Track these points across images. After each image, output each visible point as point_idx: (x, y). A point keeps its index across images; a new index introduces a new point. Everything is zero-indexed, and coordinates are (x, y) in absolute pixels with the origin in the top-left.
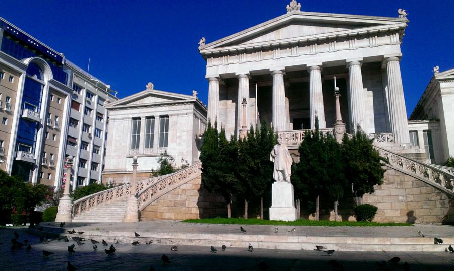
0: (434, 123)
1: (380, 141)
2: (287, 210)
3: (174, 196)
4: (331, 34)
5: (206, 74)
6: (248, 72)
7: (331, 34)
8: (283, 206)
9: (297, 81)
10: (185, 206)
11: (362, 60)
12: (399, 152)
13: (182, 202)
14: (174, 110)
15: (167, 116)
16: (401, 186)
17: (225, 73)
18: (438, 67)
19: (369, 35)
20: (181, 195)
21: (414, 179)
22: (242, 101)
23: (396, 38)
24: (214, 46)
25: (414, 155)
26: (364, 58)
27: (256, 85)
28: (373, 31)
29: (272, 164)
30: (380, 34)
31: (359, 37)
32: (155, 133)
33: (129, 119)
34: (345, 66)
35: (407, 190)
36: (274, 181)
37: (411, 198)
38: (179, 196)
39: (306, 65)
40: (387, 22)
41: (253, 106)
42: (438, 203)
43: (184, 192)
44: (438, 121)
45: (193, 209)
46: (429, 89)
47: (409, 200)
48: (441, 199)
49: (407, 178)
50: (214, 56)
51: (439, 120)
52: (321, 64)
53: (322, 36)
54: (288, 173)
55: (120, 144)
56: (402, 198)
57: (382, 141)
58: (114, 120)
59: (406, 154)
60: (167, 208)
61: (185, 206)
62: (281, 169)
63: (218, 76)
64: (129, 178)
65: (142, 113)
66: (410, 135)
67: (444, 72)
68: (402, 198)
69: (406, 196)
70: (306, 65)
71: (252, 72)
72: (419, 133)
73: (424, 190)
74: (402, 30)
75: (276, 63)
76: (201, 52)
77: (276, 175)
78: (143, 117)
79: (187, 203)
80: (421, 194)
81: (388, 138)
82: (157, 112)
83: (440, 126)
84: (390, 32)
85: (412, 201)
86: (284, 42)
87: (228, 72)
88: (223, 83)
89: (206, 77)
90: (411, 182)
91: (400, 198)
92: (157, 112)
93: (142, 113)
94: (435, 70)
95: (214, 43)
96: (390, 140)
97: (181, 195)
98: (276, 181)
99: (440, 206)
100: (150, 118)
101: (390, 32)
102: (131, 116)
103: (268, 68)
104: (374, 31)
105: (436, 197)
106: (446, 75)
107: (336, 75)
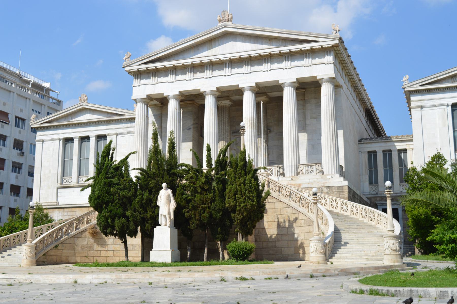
1: (309, 173)
4: (263, 51)
5: (132, 95)
7: (263, 51)
9: (230, 102)
11: (295, 80)
12: (322, 184)
13: (89, 245)
14: (112, 129)
18: (407, 76)
19: (302, 54)
21: (306, 218)
23: (330, 58)
24: (140, 63)
25: (336, 188)
26: (297, 79)
32: (90, 158)
33: (60, 140)
39: (238, 85)
41: (190, 129)
52: (254, 85)
53: (254, 53)
55: (50, 171)
57: (311, 173)
58: (43, 141)
59: (329, 187)
63: (145, 97)
64: (60, 213)
65: (76, 133)
66: (384, 154)
70: (238, 85)
72: (393, 153)
74: (336, 47)
75: (207, 83)
77: (161, 220)
78: (76, 138)
80: (309, 232)
81: (316, 169)
82: (92, 132)
84: (324, 51)
88: (155, 102)
89: (133, 97)
92: (92, 132)
93: (76, 133)
94: (404, 80)
96: (318, 171)
98: (160, 225)
100: (84, 139)
101: (324, 51)
102: (62, 136)
103: (198, 88)
104: (307, 48)
107: (270, 97)
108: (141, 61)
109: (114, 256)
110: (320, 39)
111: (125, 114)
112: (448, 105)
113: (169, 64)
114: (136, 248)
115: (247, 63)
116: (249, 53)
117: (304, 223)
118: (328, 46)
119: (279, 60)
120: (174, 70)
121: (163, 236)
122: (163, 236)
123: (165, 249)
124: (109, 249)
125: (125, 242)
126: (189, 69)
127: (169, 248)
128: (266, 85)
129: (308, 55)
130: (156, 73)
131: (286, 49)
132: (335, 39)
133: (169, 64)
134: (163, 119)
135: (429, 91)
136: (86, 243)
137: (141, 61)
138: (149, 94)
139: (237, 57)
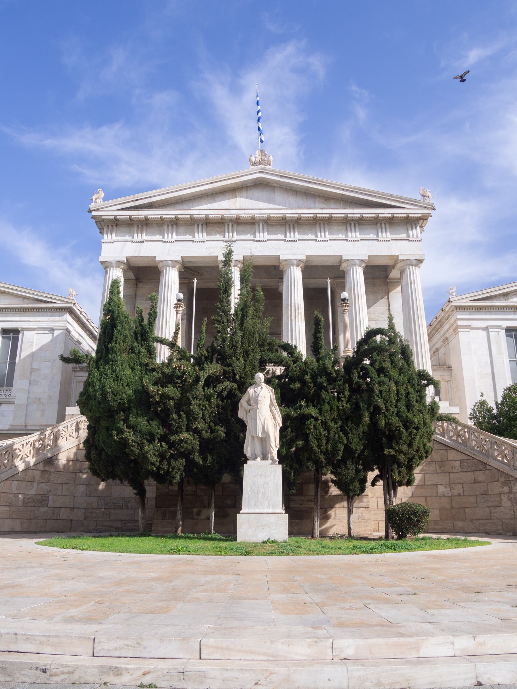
0: (444, 370)
2: (272, 518)
3: (24, 484)
4: (320, 211)
5: (100, 255)
6: (180, 259)
8: (265, 511)
10: (47, 506)
14: (30, 321)
15: (16, 331)
16: (443, 468)
17: (136, 255)
19: (377, 223)
20: (39, 483)
21: (464, 457)
22: (176, 302)
24: (120, 207)
26: (369, 256)
27: (195, 281)
28: (384, 215)
29: (243, 426)
30: (391, 222)
31: (360, 223)
34: (339, 266)
35: (451, 474)
36: (246, 460)
37: (458, 490)
38: (35, 484)
39: (279, 257)
40: (404, 206)
42: (505, 498)
43: (46, 476)
44: (449, 367)
45: (62, 510)
46: (438, 320)
47: (455, 492)
48: (510, 492)
49: (452, 455)
50: (115, 224)
51: (451, 367)
52: (303, 258)
53: (307, 212)
54: (275, 444)
56: (444, 490)
60: (7, 508)
61: (47, 506)
62: (260, 435)
67: (463, 297)
68: (444, 490)
69: (450, 485)
70: (279, 257)
71: (186, 260)
73: (481, 476)
76: (94, 213)
79: (51, 497)
80: (476, 482)
83: (451, 375)
85: (459, 495)
86: (245, 214)
87: (142, 254)
88: (131, 275)
89: (101, 259)
90: (458, 462)
91: (441, 489)
95: (120, 200)
97: (39, 483)
99: (509, 504)
104: (386, 215)
105: (503, 488)
106: (465, 300)
108: (121, 204)
109: (86, 518)
110: (404, 206)
111: (53, 301)
112: (499, 328)
113: (169, 213)
114: (130, 505)
115: (291, 226)
116: (300, 211)
117: (461, 466)
118: (417, 215)
119: (340, 228)
120: (175, 224)
121: (263, 481)
122: (263, 481)
123: (271, 511)
124: (76, 506)
125: (141, 493)
126: (198, 225)
127: (280, 508)
128: (315, 264)
129: (383, 225)
130: (144, 224)
131: (356, 212)
132: (427, 208)
133: (169, 213)
134: (137, 301)
135: (479, 309)
136: (33, 492)
137: (121, 204)
138: (130, 255)
139: (280, 215)
